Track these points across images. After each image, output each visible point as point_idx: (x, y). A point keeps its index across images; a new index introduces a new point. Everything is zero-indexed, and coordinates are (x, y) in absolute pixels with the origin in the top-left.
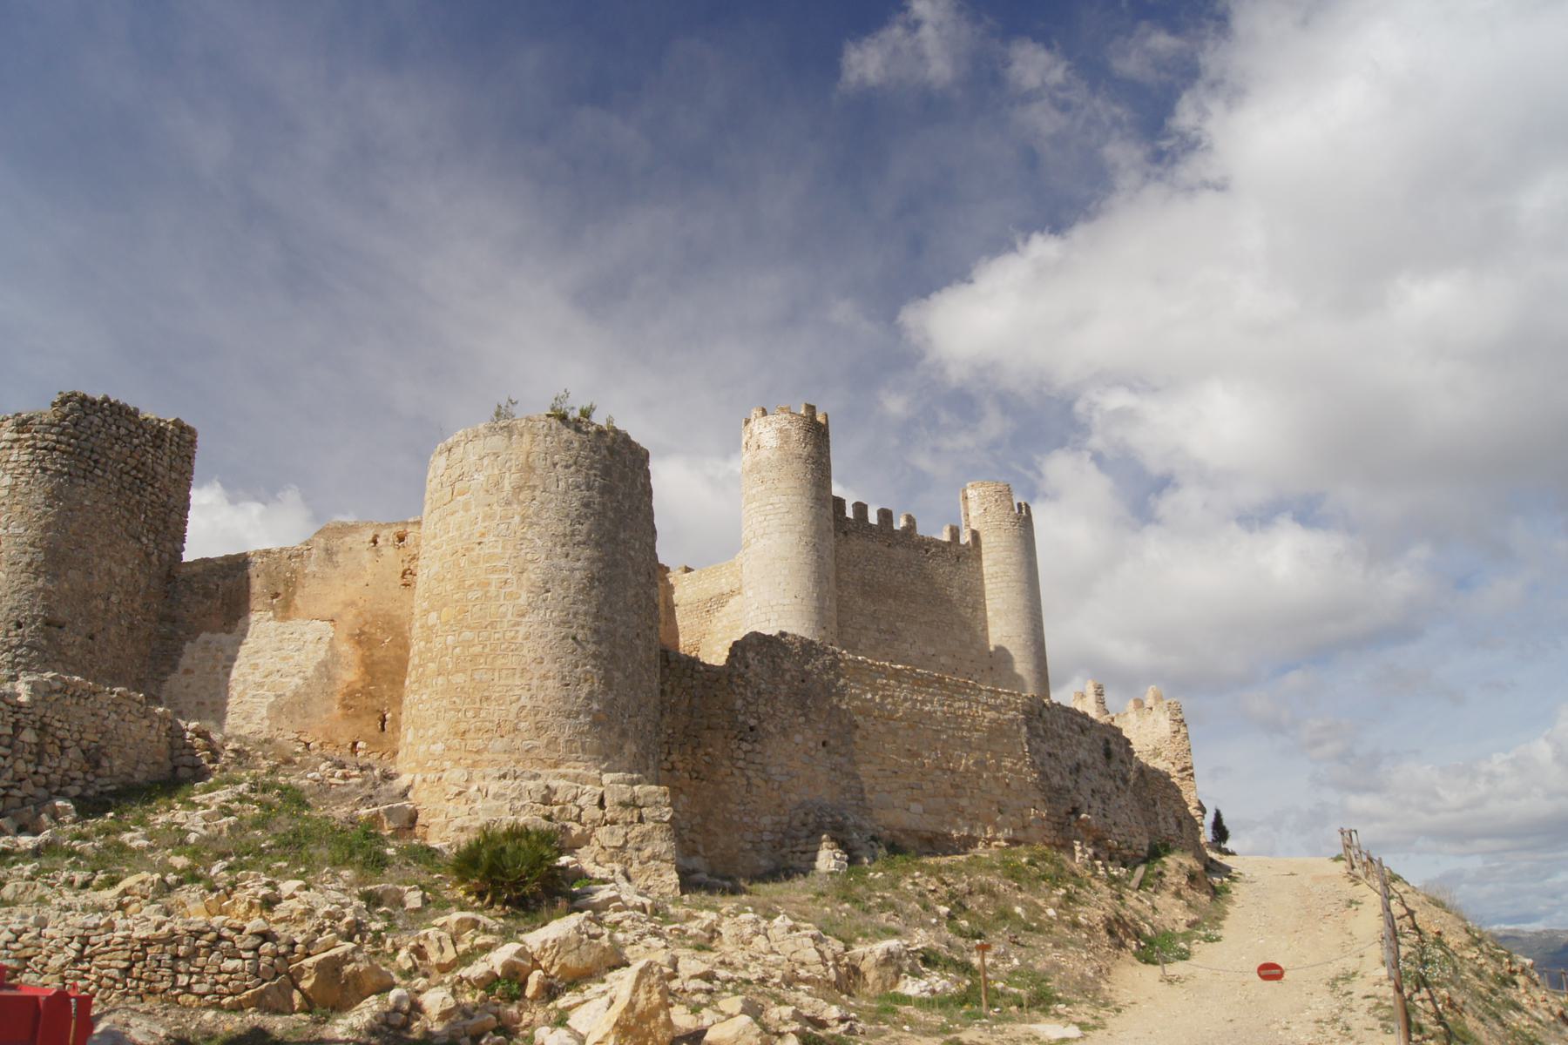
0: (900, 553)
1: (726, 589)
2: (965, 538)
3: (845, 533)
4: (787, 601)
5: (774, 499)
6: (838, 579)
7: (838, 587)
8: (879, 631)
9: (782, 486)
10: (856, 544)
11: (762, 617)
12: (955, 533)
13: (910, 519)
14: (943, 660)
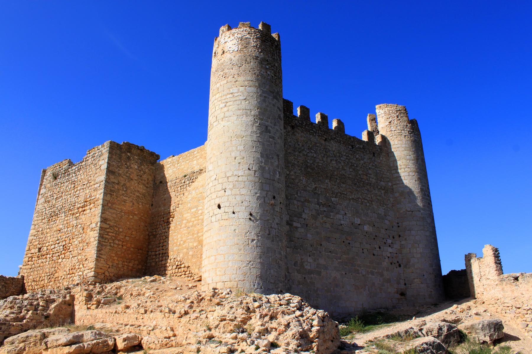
0: (333, 146)
1: (197, 169)
2: (378, 140)
3: (293, 127)
4: (240, 173)
5: (235, 90)
6: (287, 162)
7: (287, 167)
8: (318, 203)
9: (241, 79)
10: (300, 136)
11: (219, 187)
12: (371, 135)
13: (339, 122)
14: (366, 228)
